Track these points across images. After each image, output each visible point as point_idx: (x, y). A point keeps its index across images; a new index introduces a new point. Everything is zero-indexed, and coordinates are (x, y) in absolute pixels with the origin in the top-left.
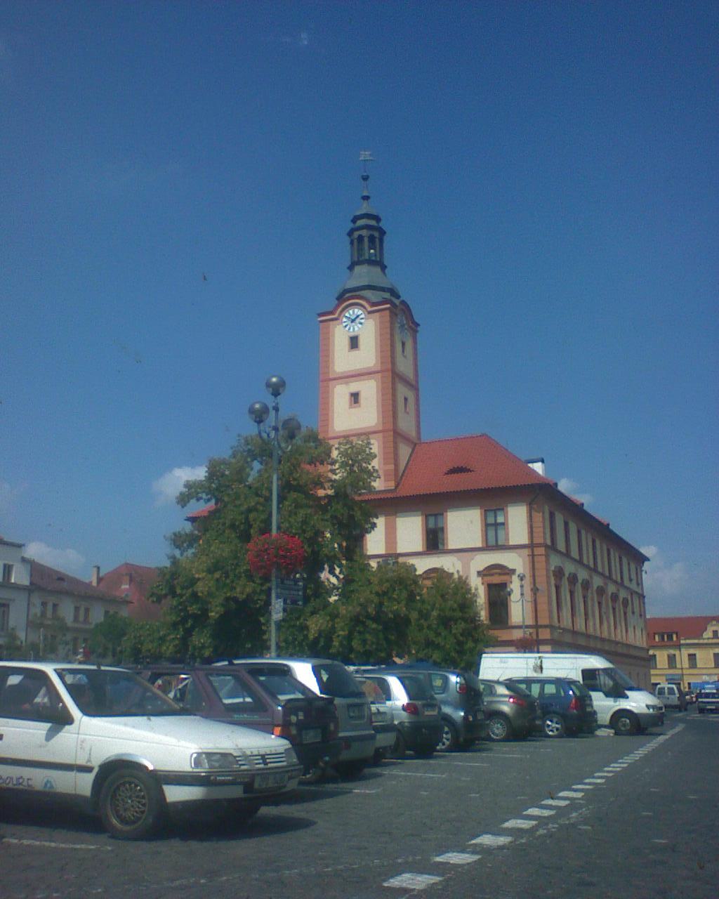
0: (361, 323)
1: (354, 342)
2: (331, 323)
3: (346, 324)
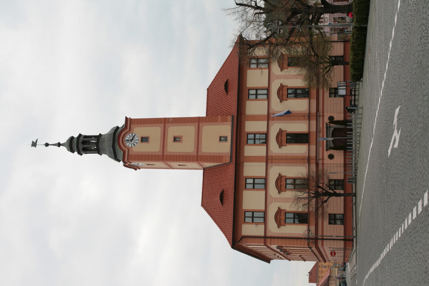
0: (135, 135)
1: (144, 140)
2: (130, 154)
3: (133, 145)
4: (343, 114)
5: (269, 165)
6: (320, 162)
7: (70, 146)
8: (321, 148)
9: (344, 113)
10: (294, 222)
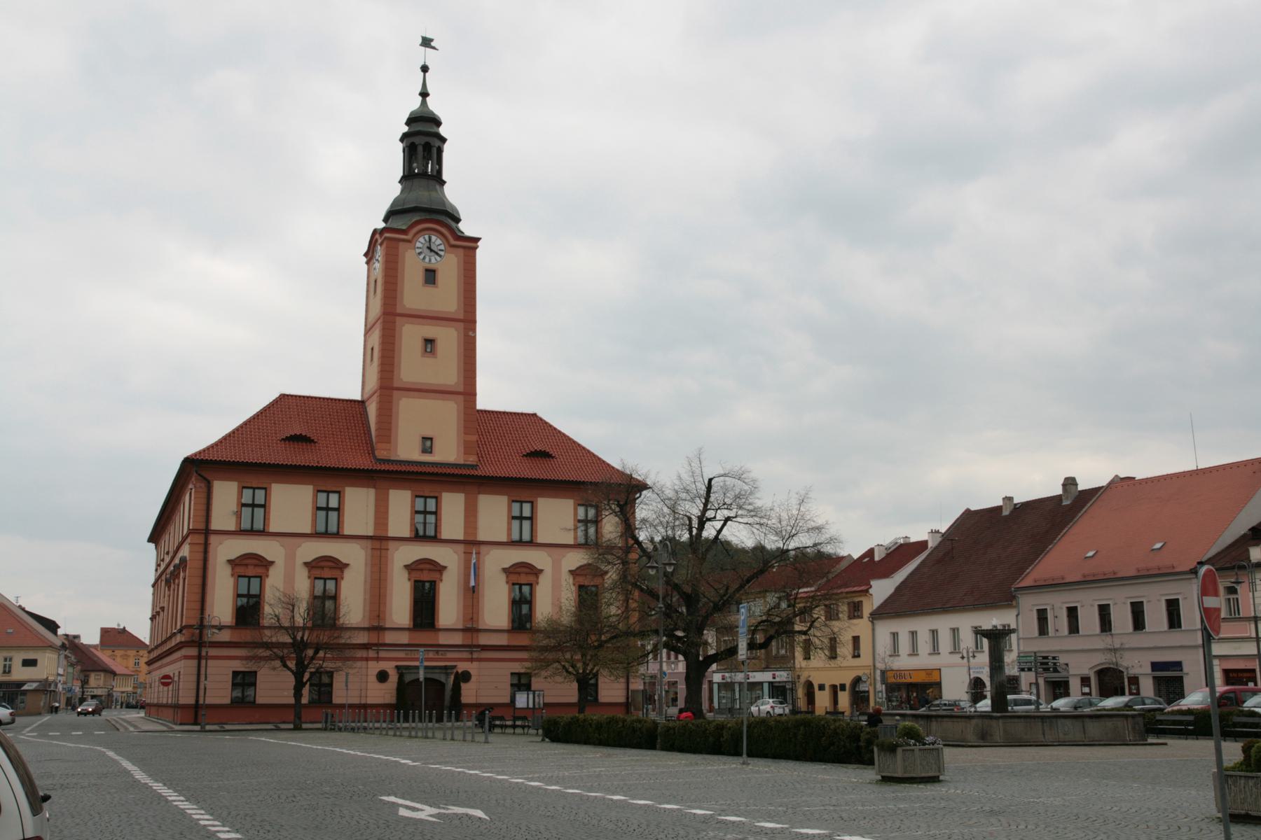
0: (440, 256)
1: (431, 276)
2: (401, 244)
3: (420, 250)
4: (475, 702)
5: (369, 543)
6: (372, 654)
7: (421, 117)
8: (402, 655)
9: (476, 704)
10: (239, 596)
